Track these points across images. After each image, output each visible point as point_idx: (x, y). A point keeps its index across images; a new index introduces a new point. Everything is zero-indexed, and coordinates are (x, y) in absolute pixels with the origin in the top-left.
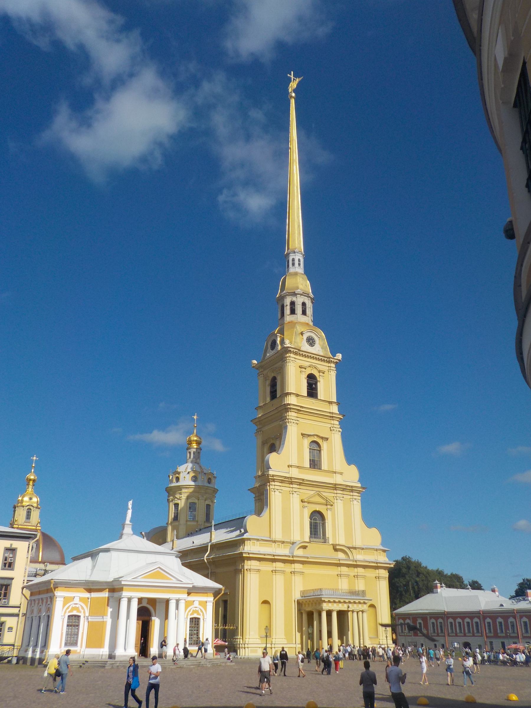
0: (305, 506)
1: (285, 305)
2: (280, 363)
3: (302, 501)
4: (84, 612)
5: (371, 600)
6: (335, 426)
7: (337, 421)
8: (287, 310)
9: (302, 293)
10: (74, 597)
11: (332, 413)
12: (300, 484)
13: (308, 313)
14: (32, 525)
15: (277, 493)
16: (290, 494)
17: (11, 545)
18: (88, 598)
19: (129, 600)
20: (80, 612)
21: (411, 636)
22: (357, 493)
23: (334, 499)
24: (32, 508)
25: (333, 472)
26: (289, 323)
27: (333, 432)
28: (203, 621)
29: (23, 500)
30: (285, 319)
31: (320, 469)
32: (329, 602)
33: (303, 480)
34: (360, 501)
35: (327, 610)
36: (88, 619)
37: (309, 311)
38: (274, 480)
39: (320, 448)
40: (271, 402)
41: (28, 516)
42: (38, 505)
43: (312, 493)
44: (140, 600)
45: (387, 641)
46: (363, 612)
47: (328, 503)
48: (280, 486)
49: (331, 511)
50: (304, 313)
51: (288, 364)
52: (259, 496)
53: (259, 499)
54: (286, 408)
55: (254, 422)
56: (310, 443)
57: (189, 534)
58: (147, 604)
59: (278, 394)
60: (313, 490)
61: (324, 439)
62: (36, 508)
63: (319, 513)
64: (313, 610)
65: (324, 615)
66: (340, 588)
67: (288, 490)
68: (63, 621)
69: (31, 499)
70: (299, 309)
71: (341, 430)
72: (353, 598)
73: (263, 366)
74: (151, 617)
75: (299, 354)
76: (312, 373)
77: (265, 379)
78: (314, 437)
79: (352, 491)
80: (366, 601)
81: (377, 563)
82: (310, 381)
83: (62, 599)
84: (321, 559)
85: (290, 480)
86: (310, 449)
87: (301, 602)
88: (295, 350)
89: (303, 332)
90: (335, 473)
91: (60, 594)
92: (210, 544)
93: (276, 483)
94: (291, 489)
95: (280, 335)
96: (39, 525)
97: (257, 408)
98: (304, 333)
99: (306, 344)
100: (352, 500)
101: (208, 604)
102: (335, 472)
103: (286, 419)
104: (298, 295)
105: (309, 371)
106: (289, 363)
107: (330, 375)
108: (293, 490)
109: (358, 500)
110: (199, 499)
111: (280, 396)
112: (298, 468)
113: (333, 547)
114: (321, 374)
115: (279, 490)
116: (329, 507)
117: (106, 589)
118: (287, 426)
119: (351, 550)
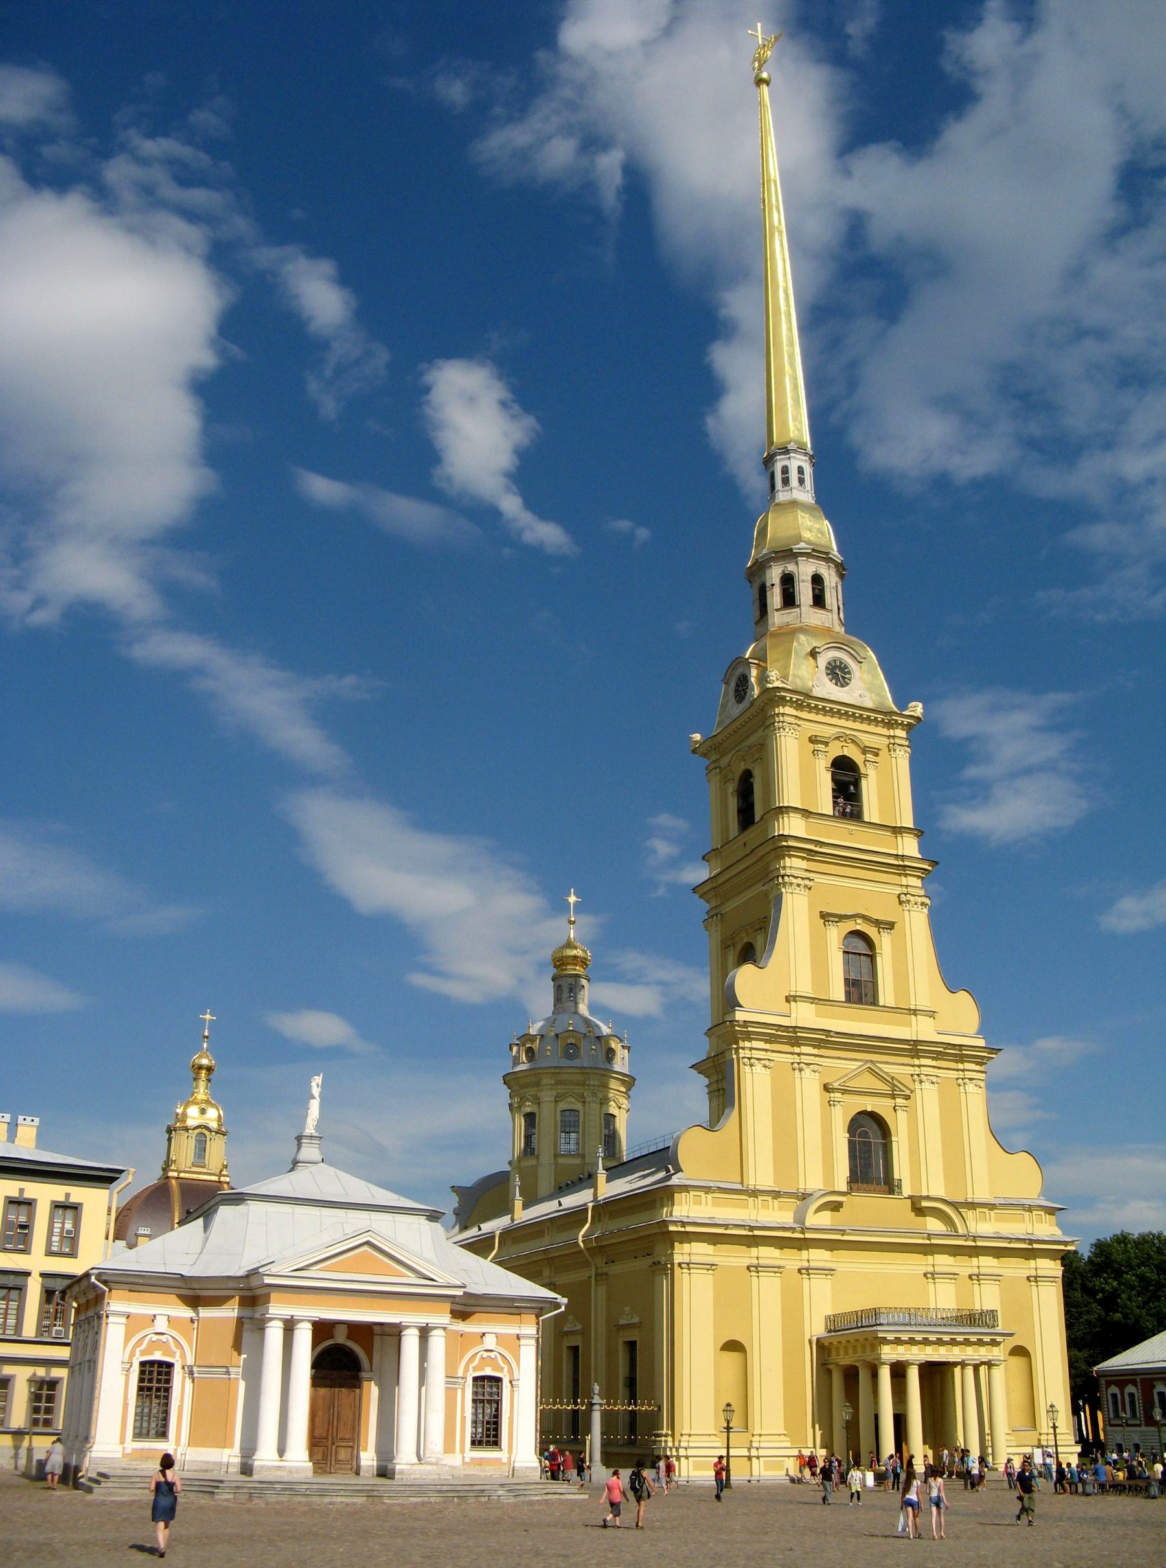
0: (834, 1101)
1: (768, 584)
2: (760, 733)
3: (827, 1088)
4: (183, 1355)
5: (1011, 1335)
6: (910, 890)
7: (915, 879)
8: (775, 598)
9: (810, 551)
10: (155, 1316)
11: (903, 856)
12: (819, 1044)
13: (829, 602)
14: (208, 1171)
15: (758, 1068)
16: (794, 1069)
17: (68, 1195)
18: (192, 1321)
19: (289, 1326)
20: (173, 1354)
21: (1139, 1425)
22: (977, 1063)
23: (914, 1081)
25: (909, 1010)
26: (780, 628)
27: (908, 908)
28: (509, 1385)
29: (186, 1115)
30: (770, 621)
31: (874, 1002)
32: (898, 1341)
34: (982, 1084)
35: (893, 1363)
36: (191, 1373)
37: (832, 597)
38: (748, 1037)
39: (872, 952)
40: (739, 838)
41: (201, 1150)
42: (221, 1125)
43: (855, 1067)
44: (322, 1329)
45: (1055, 1437)
46: (990, 1364)
47: (896, 1091)
48: (766, 1050)
49: (906, 1111)
50: (819, 601)
51: (778, 735)
52: (717, 1081)
53: (719, 1090)
54: (779, 847)
55: (702, 892)
56: (845, 937)
57: (560, 1188)
58: (348, 1338)
59: (757, 818)
60: (855, 1060)
61: (882, 926)
62: (216, 1133)
63: (875, 1118)
64: (857, 1364)
65: (885, 1374)
66: (932, 1306)
67: (787, 1060)
68: (127, 1377)
69: (203, 1111)
70: (805, 593)
71: (927, 901)
72: (961, 1330)
73: (718, 747)
74: (359, 1373)
75: (809, 705)
76: (845, 754)
77: (725, 780)
78: (855, 920)
79: (961, 1058)
80: (999, 1339)
81: (1031, 1241)
82: (839, 777)
83: (123, 1320)
84: (871, 1236)
85: (791, 1034)
86: (844, 952)
87: (826, 1344)
88: (795, 697)
89: (817, 650)
90: (915, 1012)
91: (117, 1304)
92: (590, 1205)
93: (756, 1044)
94: (796, 1059)
95: (757, 662)
96: (224, 1173)
97: (706, 857)
98: (819, 653)
99: (826, 680)
100: (960, 1082)
101: (522, 1342)
102: (915, 1010)
103: (778, 877)
104: (799, 558)
105: (835, 750)
106: (781, 730)
107: (893, 759)
108: (802, 1061)
109: (979, 1082)
110: (584, 1102)
111: (762, 819)
112: (812, 1003)
113: (913, 1204)
114: (870, 757)
115: (763, 1062)
116: (900, 1101)
117: (233, 1297)
118: (782, 893)
119: (960, 1210)
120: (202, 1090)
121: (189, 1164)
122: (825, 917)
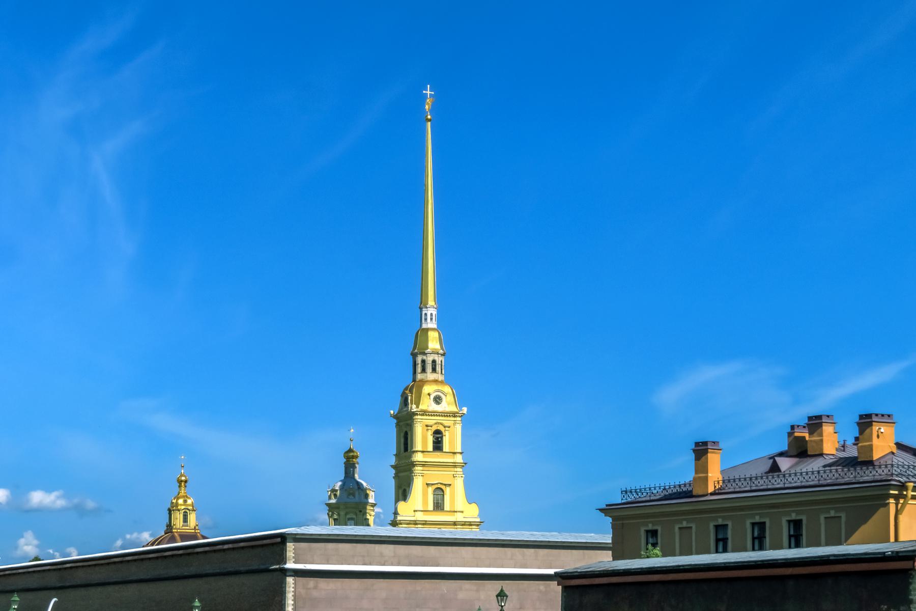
8: (419, 369)
12: (423, 524)
24: (188, 511)
29: (178, 503)
31: (443, 509)
33: (426, 521)
37: (438, 368)
41: (185, 519)
70: (429, 368)
76: (438, 428)
86: (434, 494)
90: (456, 512)
105: (434, 428)
114: (447, 429)
120: (183, 492)
121: (181, 525)
122: (427, 484)
